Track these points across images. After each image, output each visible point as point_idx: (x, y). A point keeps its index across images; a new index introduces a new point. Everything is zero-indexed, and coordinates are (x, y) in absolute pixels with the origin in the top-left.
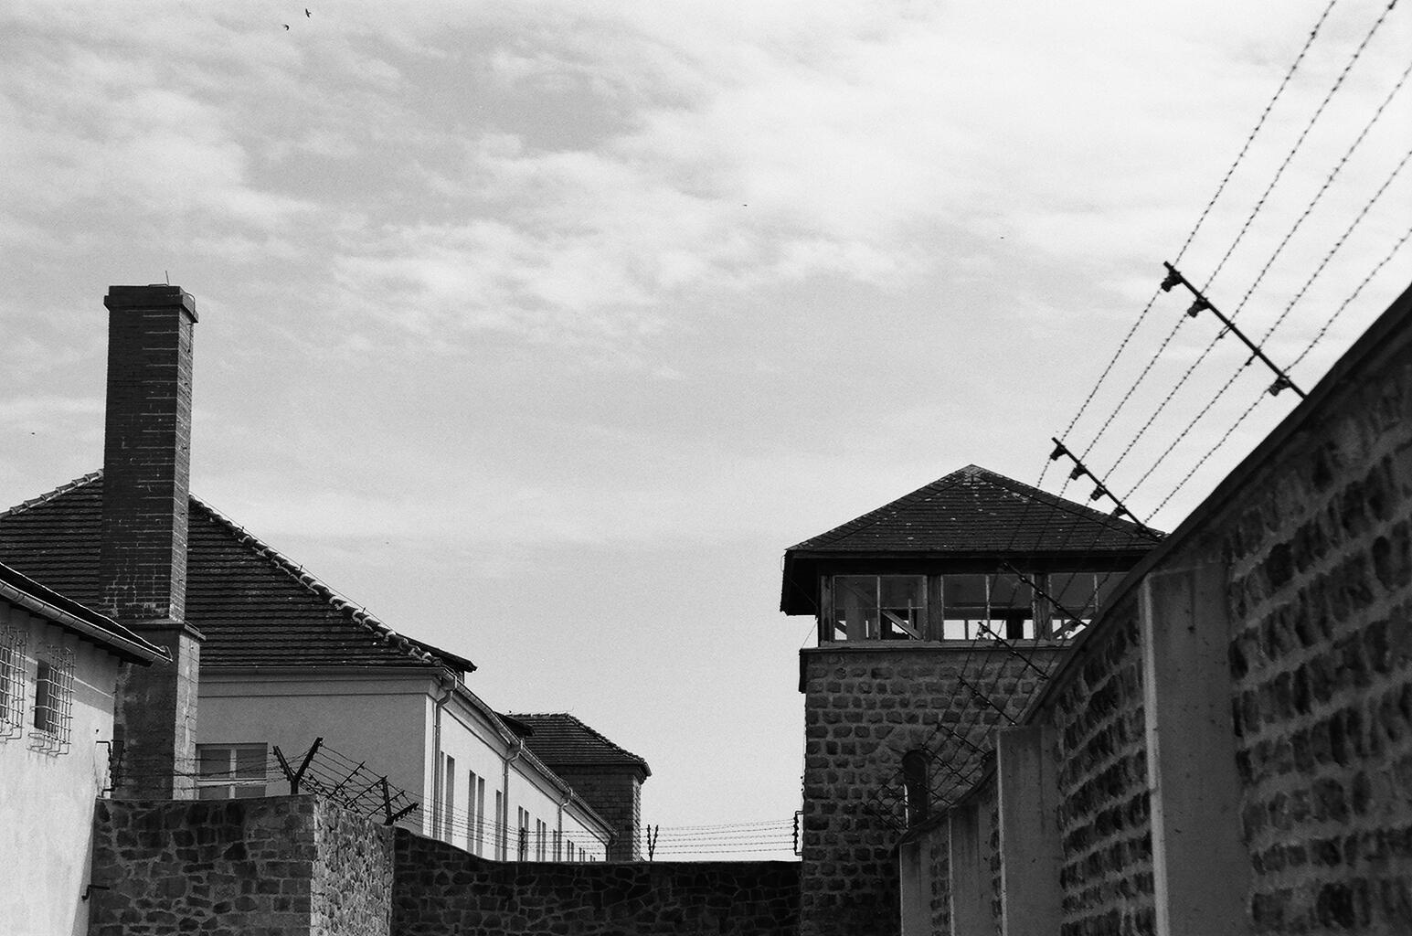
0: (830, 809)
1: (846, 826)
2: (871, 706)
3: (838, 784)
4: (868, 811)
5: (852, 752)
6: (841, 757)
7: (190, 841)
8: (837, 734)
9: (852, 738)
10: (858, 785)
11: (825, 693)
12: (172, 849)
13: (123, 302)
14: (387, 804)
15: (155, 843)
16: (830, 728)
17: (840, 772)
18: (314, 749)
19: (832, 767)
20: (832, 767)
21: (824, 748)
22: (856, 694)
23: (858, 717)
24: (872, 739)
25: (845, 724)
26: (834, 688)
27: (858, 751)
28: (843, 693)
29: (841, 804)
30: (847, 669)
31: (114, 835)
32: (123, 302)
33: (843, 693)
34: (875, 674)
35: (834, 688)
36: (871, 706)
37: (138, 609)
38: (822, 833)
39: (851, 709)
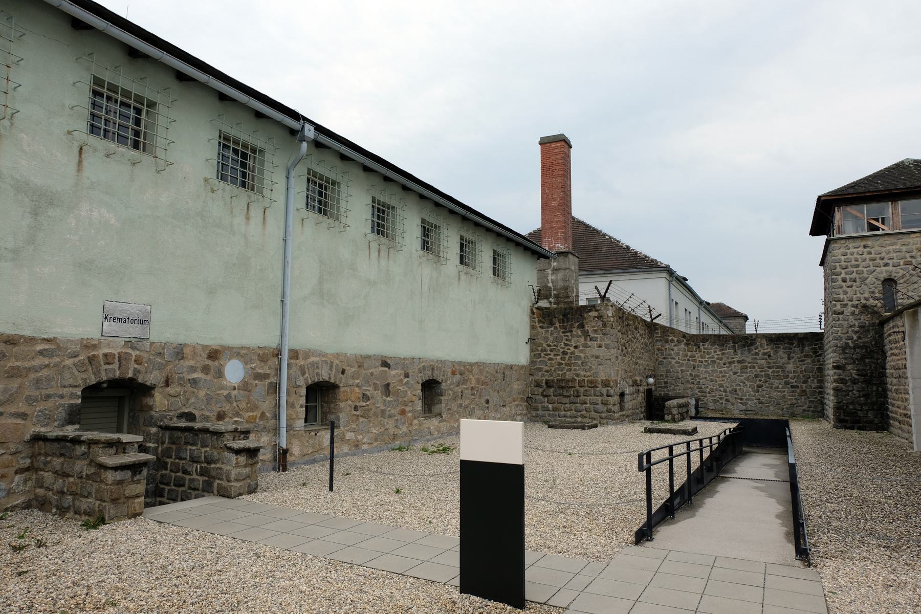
0: (846, 305)
1: (853, 314)
2: (864, 260)
3: (848, 295)
4: (865, 306)
5: (855, 281)
6: (849, 284)
7: (564, 322)
8: (846, 273)
9: (854, 275)
10: (858, 295)
11: (840, 257)
12: (557, 325)
13: (545, 142)
14: (650, 311)
15: (551, 324)
16: (843, 271)
17: (849, 290)
18: (609, 285)
19: (845, 288)
20: (845, 288)
21: (840, 280)
22: (855, 256)
23: (857, 266)
24: (865, 275)
25: (850, 269)
26: (845, 254)
27: (858, 280)
28: (849, 256)
29: (850, 303)
30: (851, 245)
31: (536, 320)
32: (545, 142)
33: (849, 256)
34: (865, 247)
35: (845, 254)
36: (864, 260)
37: (554, 247)
38: (841, 316)
39: (853, 262)
